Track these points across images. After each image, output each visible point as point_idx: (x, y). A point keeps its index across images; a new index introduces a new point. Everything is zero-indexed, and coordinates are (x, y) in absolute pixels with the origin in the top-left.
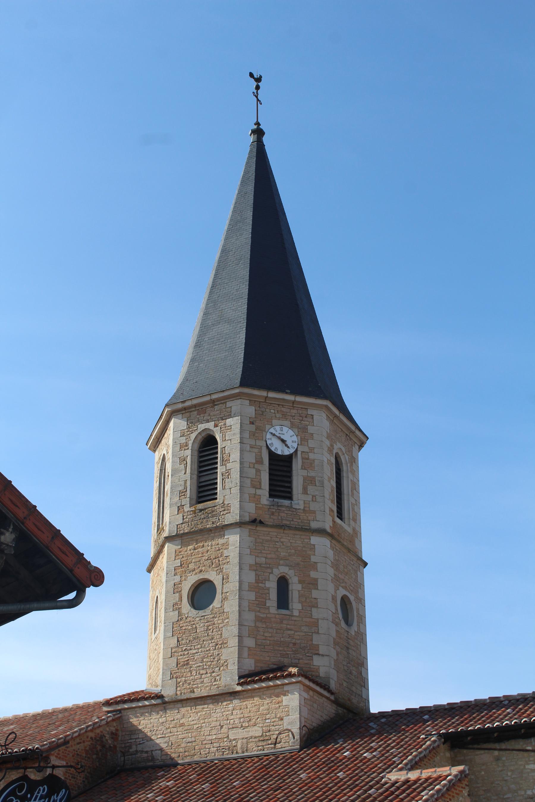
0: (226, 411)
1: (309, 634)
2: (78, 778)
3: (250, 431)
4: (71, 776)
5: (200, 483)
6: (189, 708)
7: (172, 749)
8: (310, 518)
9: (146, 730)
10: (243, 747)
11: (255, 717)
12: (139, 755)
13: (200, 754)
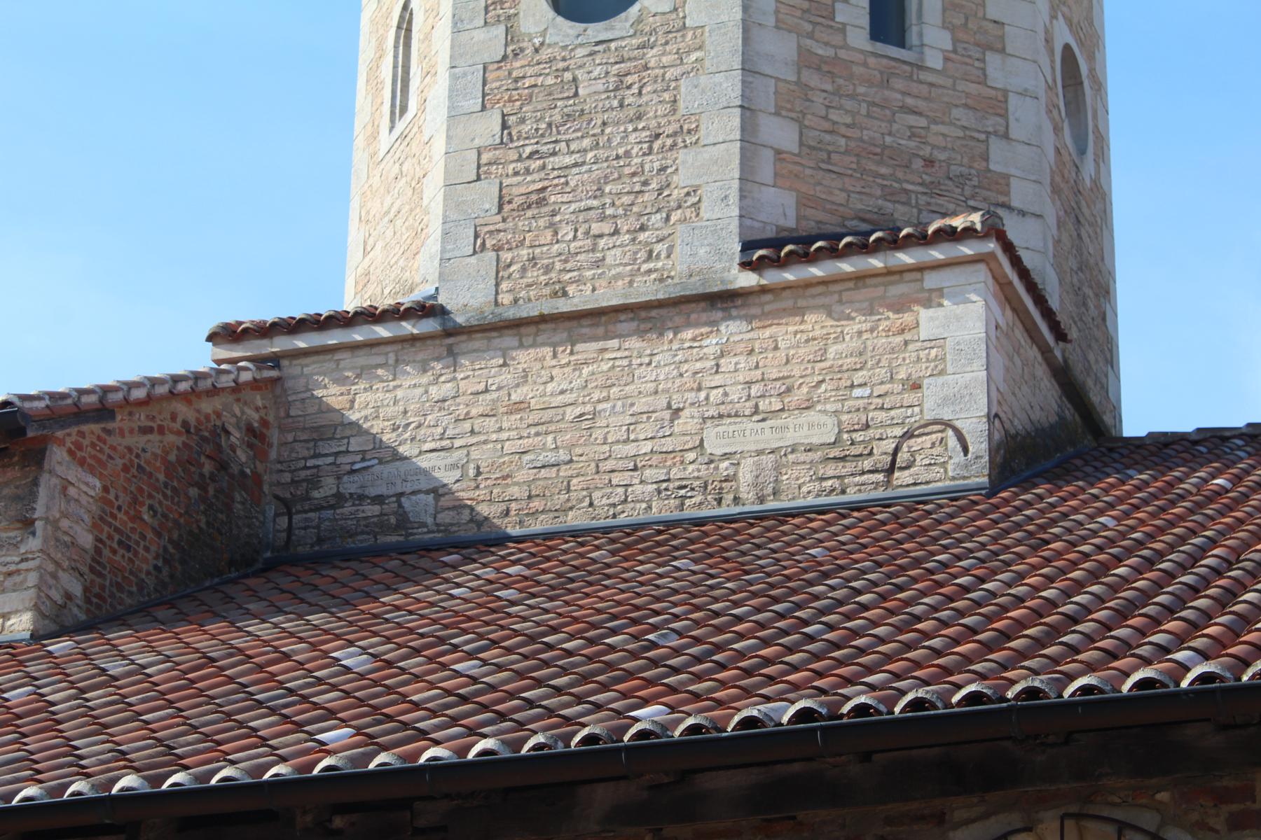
1: (976, 135)
2: (141, 551)
4: (117, 537)
6: (548, 351)
7: (477, 487)
9: (376, 427)
10: (760, 480)
11: (808, 380)
12: (348, 509)
13: (591, 505)
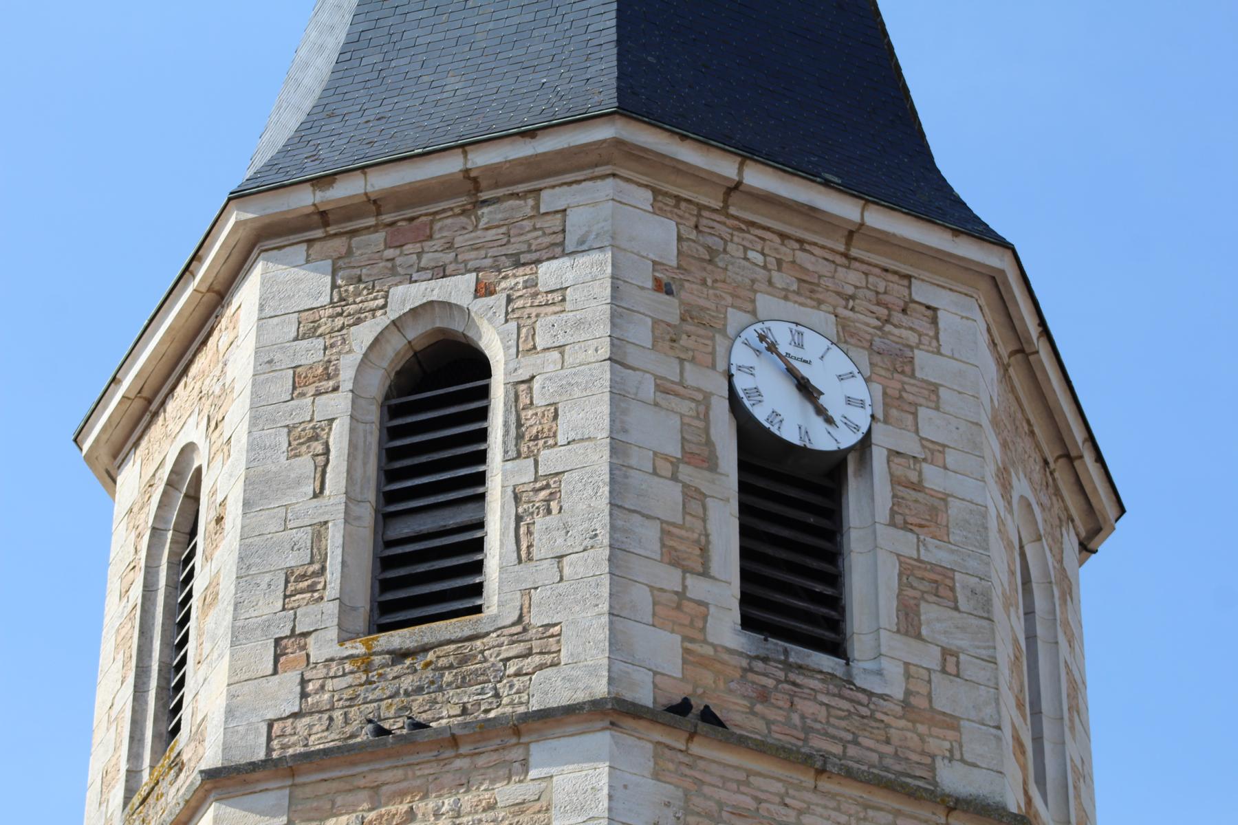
0: (535, 229)
3: (656, 322)
5: (389, 544)
8: (933, 745)
